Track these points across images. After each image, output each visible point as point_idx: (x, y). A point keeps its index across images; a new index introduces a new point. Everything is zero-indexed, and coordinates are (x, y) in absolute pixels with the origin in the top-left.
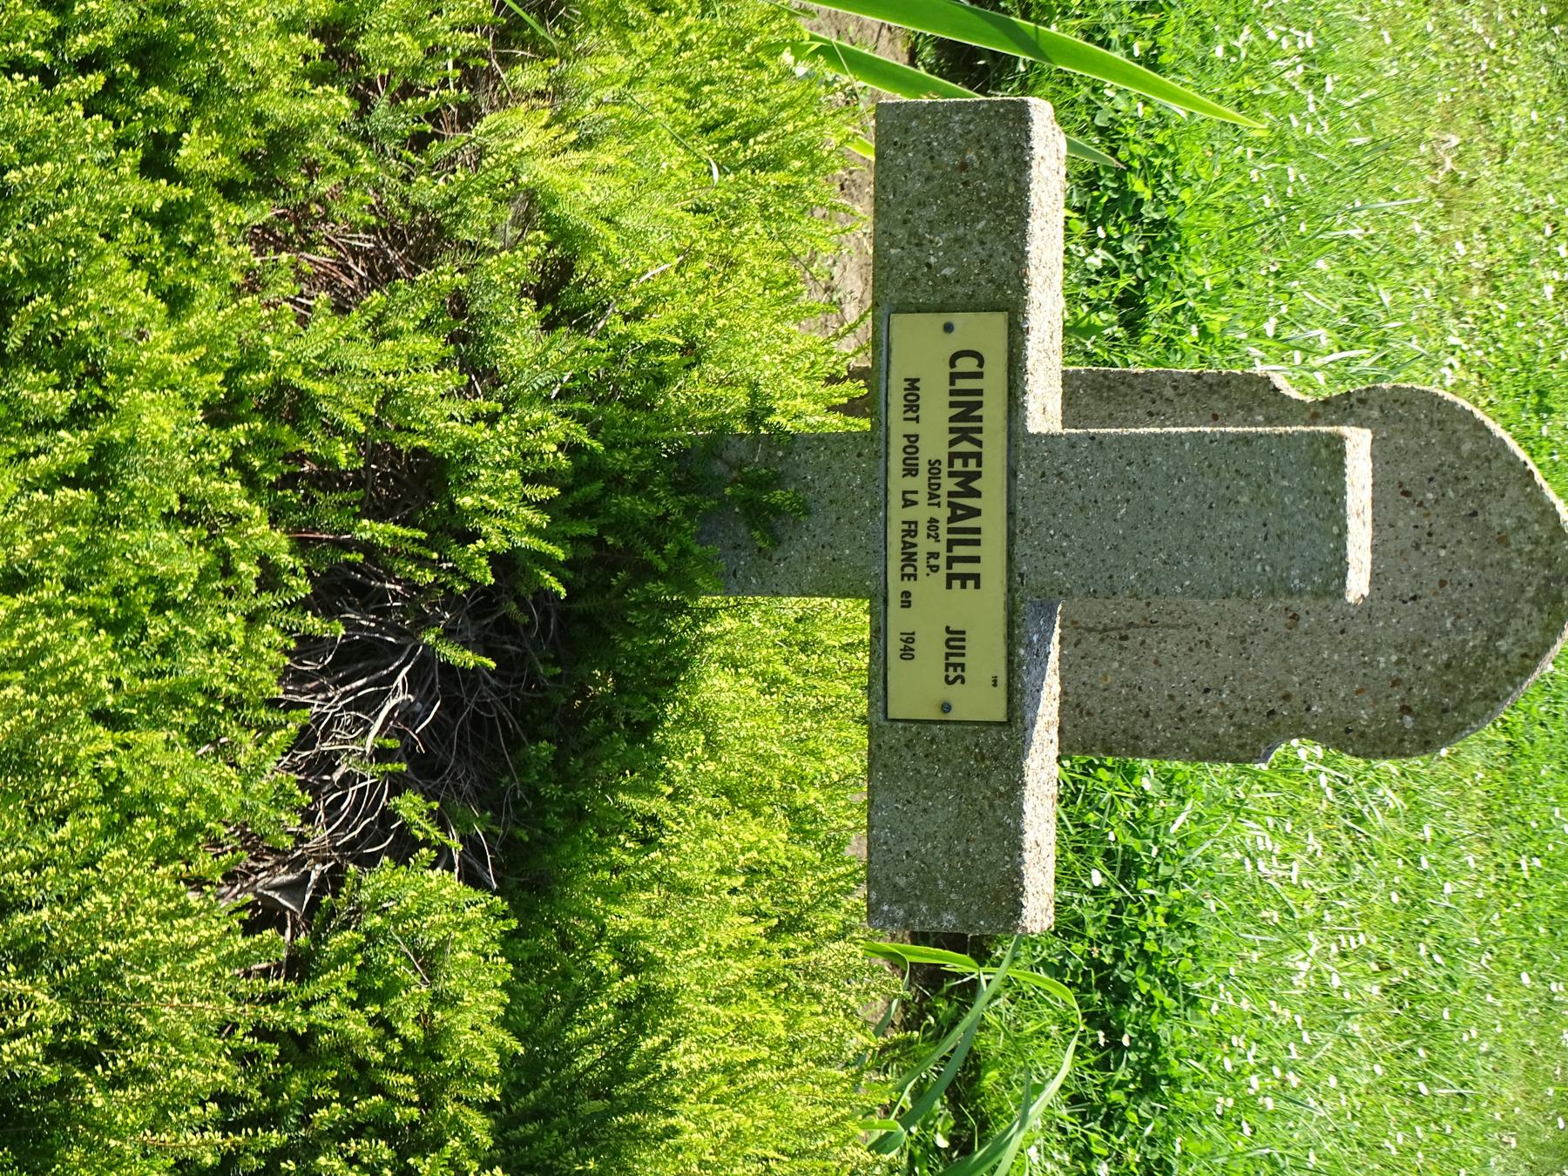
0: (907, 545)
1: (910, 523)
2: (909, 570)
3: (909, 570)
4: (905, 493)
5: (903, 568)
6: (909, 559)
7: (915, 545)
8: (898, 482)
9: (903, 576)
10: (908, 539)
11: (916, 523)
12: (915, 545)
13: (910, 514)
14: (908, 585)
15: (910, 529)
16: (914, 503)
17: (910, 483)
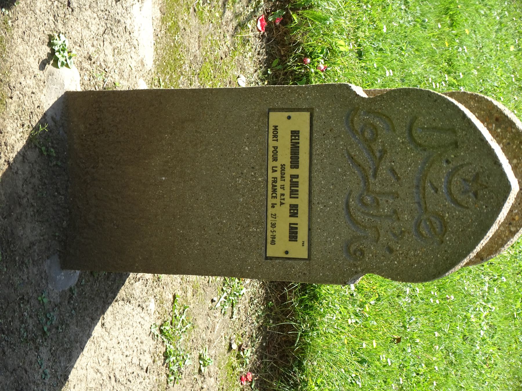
0: (274, 186)
1: (274, 178)
2: (274, 195)
3: (274, 195)
4: (273, 167)
5: (272, 194)
6: (274, 191)
7: (276, 186)
8: (271, 164)
9: (272, 197)
10: (274, 184)
11: (276, 178)
12: (276, 186)
13: (275, 175)
14: (274, 201)
15: (275, 180)
16: (276, 171)
17: (275, 164)
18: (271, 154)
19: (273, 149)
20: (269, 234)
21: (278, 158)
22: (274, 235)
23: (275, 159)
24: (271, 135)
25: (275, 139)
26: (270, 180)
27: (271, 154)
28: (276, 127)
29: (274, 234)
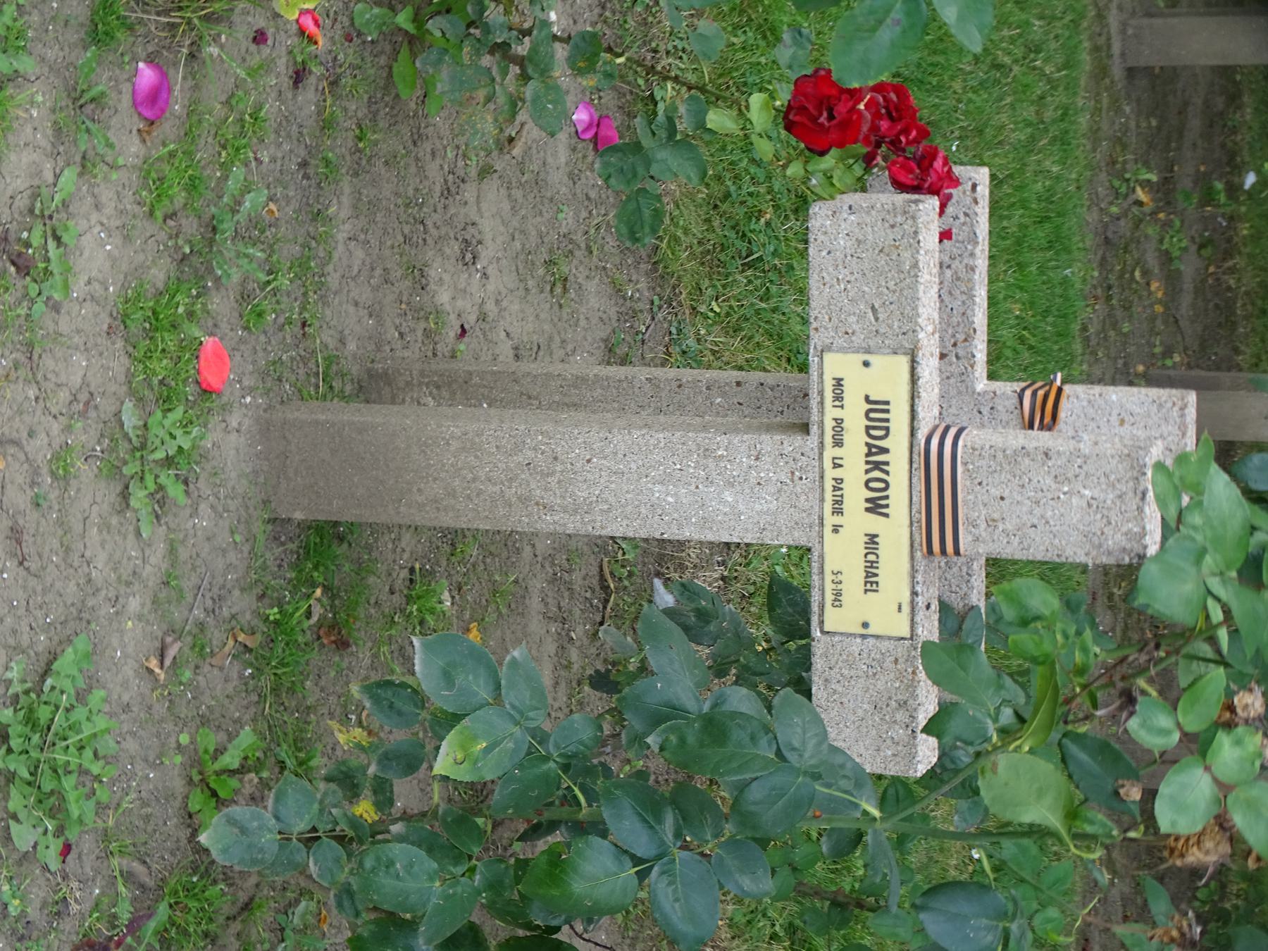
8: (830, 452)
13: (838, 473)
16: (841, 466)
17: (838, 452)
18: (829, 433)
19: (834, 424)
20: (829, 587)
21: (845, 442)
22: (840, 587)
23: (838, 443)
24: (829, 395)
25: (837, 403)
26: (829, 484)
27: (829, 433)
28: (839, 382)
29: (840, 587)
